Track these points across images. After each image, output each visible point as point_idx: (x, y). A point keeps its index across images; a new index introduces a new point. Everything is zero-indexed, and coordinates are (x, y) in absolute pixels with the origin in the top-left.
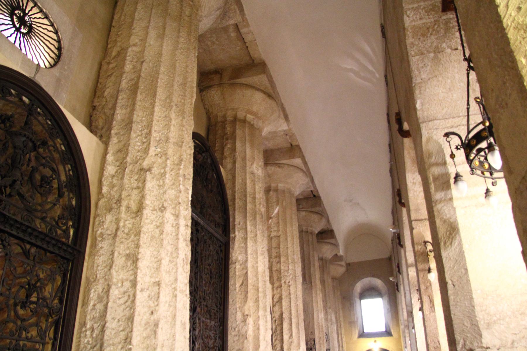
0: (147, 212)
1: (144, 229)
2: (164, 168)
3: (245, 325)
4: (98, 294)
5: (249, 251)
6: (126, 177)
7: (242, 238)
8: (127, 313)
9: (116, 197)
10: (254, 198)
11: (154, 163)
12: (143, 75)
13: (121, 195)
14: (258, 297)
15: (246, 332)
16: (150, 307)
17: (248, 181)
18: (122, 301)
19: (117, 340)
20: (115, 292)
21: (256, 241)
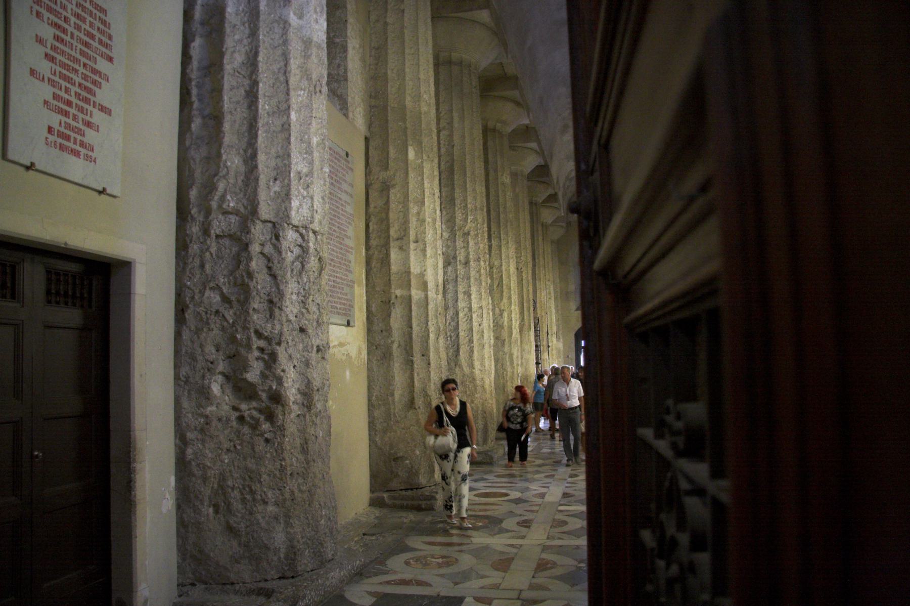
0: (472, 263)
1: (471, 275)
2: (477, 230)
3: (502, 317)
4: (451, 317)
5: (503, 257)
6: (457, 241)
7: (497, 246)
8: (468, 326)
9: (453, 254)
10: (505, 208)
11: (470, 227)
12: (455, 158)
13: (455, 254)
14: (511, 295)
15: (503, 323)
16: (478, 322)
17: (500, 192)
18: (465, 320)
19: (465, 342)
20: (461, 315)
21: (508, 248)
